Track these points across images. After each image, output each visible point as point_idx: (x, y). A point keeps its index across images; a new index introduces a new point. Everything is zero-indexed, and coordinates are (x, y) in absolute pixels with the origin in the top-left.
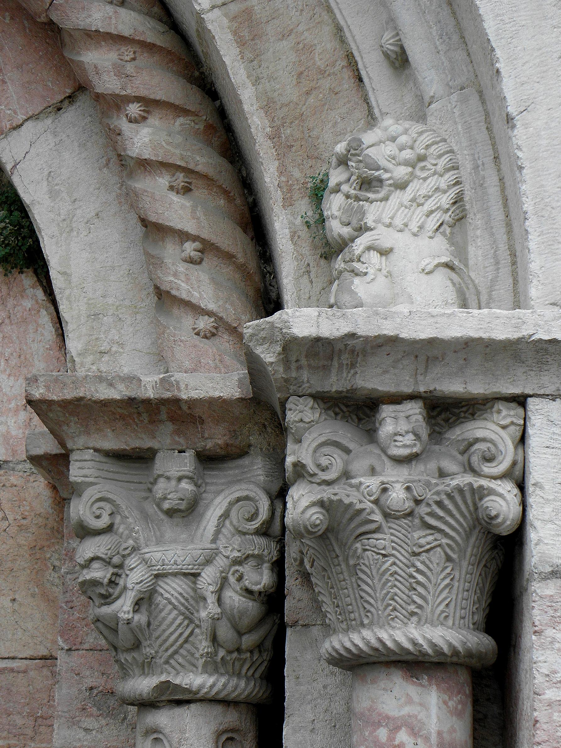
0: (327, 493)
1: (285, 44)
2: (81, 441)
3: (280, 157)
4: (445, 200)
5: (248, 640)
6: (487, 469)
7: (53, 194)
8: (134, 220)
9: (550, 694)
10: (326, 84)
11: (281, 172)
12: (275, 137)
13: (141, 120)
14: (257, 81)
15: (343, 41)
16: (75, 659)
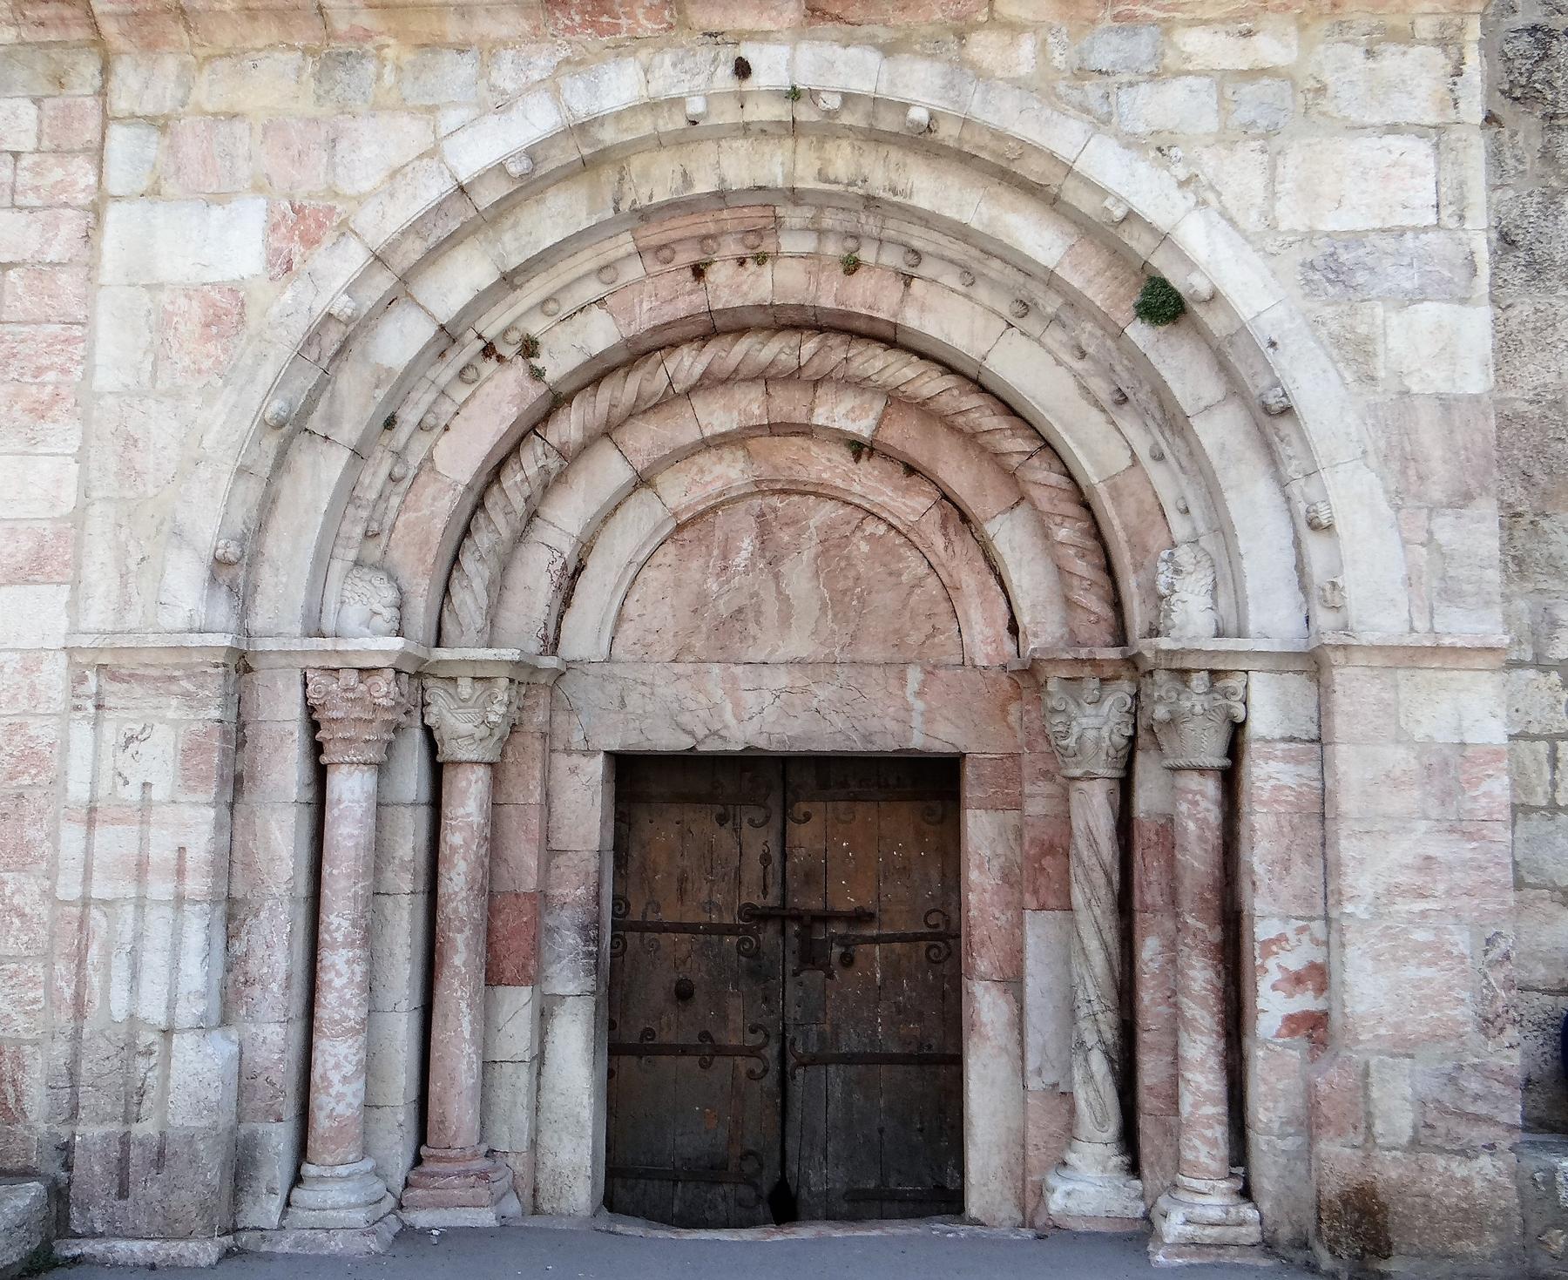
0: (1171, 708)
1: (1132, 499)
2: (1053, 674)
3: (1131, 550)
4: (1210, 579)
5: (1120, 754)
6: (1234, 698)
7: (1013, 549)
8: (1051, 567)
9: (1258, 784)
10: (1150, 517)
11: (1132, 557)
12: (1128, 541)
13: (1061, 525)
14: (1119, 516)
15: (1157, 497)
16: (1032, 757)
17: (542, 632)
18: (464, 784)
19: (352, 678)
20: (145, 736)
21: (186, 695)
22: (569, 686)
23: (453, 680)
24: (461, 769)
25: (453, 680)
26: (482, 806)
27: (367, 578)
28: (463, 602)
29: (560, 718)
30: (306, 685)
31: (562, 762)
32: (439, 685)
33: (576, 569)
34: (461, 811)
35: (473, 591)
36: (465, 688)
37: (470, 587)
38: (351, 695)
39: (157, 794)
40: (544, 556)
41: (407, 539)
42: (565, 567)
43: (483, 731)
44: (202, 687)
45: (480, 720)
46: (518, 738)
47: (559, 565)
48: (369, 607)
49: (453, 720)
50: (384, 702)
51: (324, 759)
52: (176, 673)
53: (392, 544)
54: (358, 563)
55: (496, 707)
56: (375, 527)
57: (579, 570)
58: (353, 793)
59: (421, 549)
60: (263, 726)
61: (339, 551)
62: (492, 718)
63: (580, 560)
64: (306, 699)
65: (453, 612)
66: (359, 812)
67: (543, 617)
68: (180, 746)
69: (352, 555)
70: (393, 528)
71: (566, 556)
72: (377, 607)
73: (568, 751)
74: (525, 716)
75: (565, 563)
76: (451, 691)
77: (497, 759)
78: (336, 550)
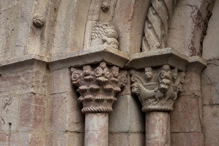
17: (191, 46)
18: (153, 122)
19: (88, 70)
20: (10, 102)
21: (23, 83)
22: (210, 72)
23: (142, 70)
24: (151, 114)
25: (142, 70)
26: (163, 133)
27: (100, 25)
28: (149, 35)
29: (206, 89)
30: (71, 75)
31: (208, 111)
32: (137, 73)
33: (207, 16)
34: (152, 136)
35: (153, 29)
36: (149, 72)
37: (151, 28)
38: (88, 77)
39: (13, 127)
40: (189, 10)
41: (121, 9)
42: (199, 14)
43: (159, 94)
44: (27, 79)
45: (158, 88)
46: (182, 99)
47: (196, 13)
48: (101, 39)
49: (145, 89)
50: (102, 79)
51: (84, 109)
52: (20, 74)
53: (115, 13)
54: (98, 21)
55: (165, 80)
56: (105, 4)
57: (209, 15)
58: (93, 127)
59: (126, 12)
60: (55, 96)
61: (89, 17)
62: (163, 86)
63: (209, 13)
64: (72, 81)
65: (145, 40)
66: (97, 136)
67: (191, 39)
68: (20, 106)
69: (96, 17)
70: (115, 7)
71: (199, 8)
72: (106, 38)
73: (212, 105)
74: (185, 87)
75: (199, 12)
76: (143, 75)
77: (172, 108)
78: (89, 17)
